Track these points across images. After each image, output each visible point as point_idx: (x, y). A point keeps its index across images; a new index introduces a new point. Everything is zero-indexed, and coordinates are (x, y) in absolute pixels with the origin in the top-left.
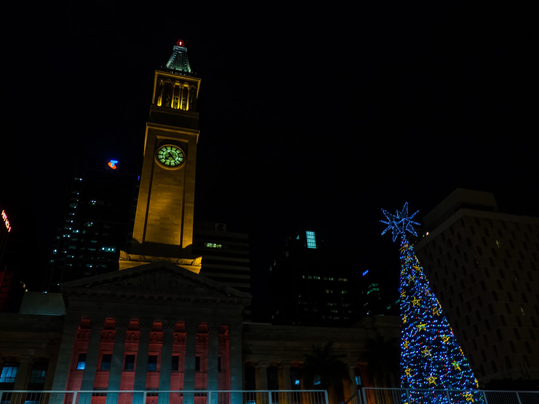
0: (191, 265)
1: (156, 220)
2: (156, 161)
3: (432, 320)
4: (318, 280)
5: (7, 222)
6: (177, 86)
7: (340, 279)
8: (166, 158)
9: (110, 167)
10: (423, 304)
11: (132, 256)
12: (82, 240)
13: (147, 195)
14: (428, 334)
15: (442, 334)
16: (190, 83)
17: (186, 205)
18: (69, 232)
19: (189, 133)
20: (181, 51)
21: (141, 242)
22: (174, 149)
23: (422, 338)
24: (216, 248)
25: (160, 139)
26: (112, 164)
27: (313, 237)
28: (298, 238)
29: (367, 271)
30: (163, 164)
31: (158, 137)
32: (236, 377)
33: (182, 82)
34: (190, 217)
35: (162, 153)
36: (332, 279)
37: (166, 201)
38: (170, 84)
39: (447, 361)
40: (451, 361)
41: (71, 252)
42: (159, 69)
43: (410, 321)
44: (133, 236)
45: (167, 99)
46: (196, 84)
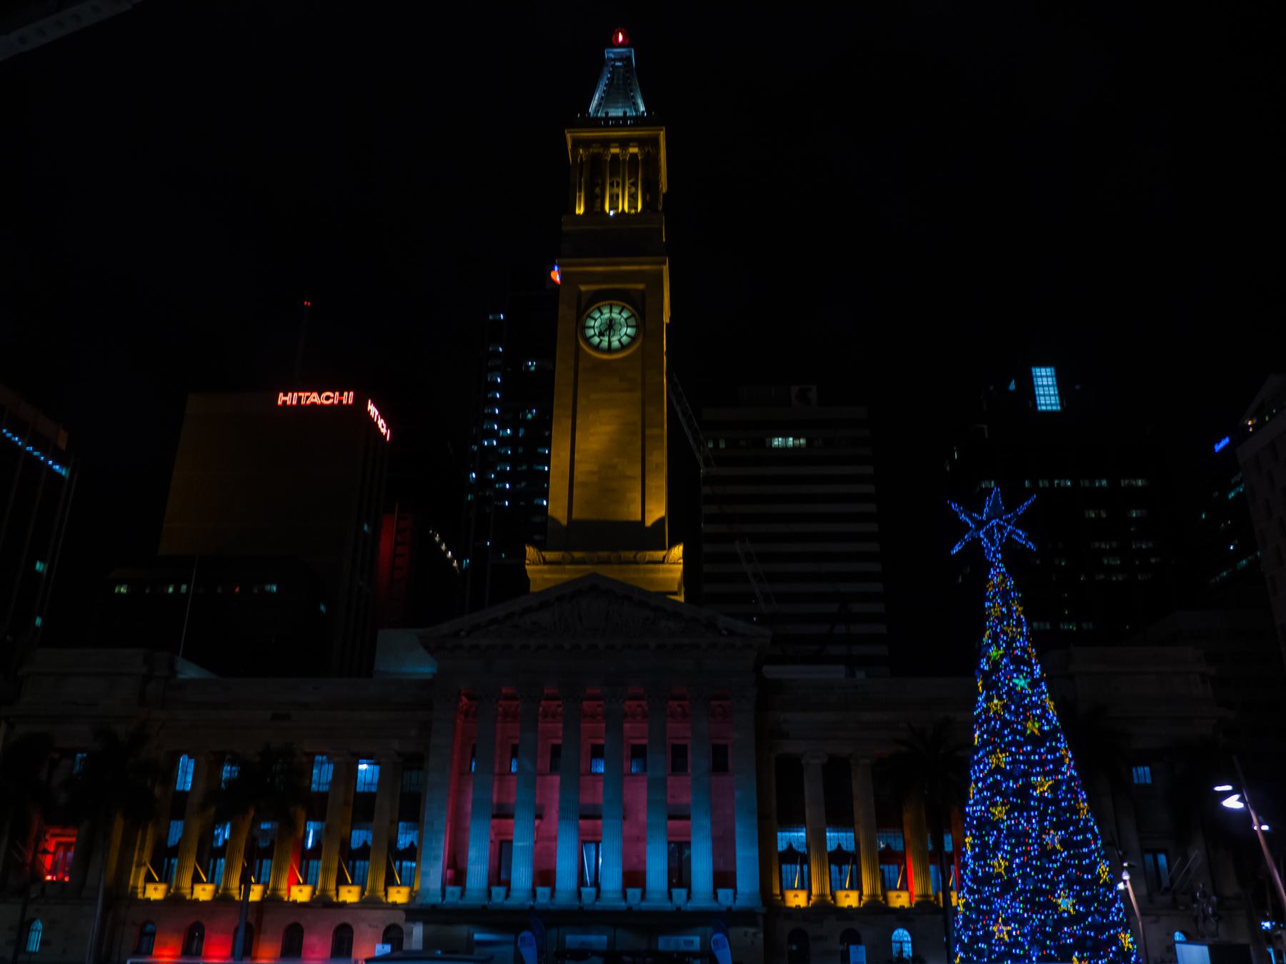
0: (663, 562)
3: (1019, 745)
4: (1066, 487)
5: (381, 422)
6: (615, 156)
7: (1124, 483)
8: (601, 334)
10: (1010, 712)
11: (549, 555)
12: (520, 450)
13: (569, 422)
14: (1007, 775)
15: (1037, 775)
16: (640, 142)
17: (648, 432)
18: (494, 434)
20: (620, 60)
21: (564, 522)
22: (616, 310)
23: (996, 782)
24: (794, 448)
25: (587, 292)
27: (1051, 381)
28: (1012, 386)
29: (1227, 440)
30: (597, 348)
31: (583, 288)
32: (742, 791)
33: (624, 143)
34: (659, 457)
35: (592, 323)
36: (1104, 483)
37: (607, 429)
39: (1034, 830)
40: (1044, 830)
41: (502, 477)
42: (574, 125)
43: (984, 743)
44: (550, 512)
45: (598, 190)
46: (654, 142)
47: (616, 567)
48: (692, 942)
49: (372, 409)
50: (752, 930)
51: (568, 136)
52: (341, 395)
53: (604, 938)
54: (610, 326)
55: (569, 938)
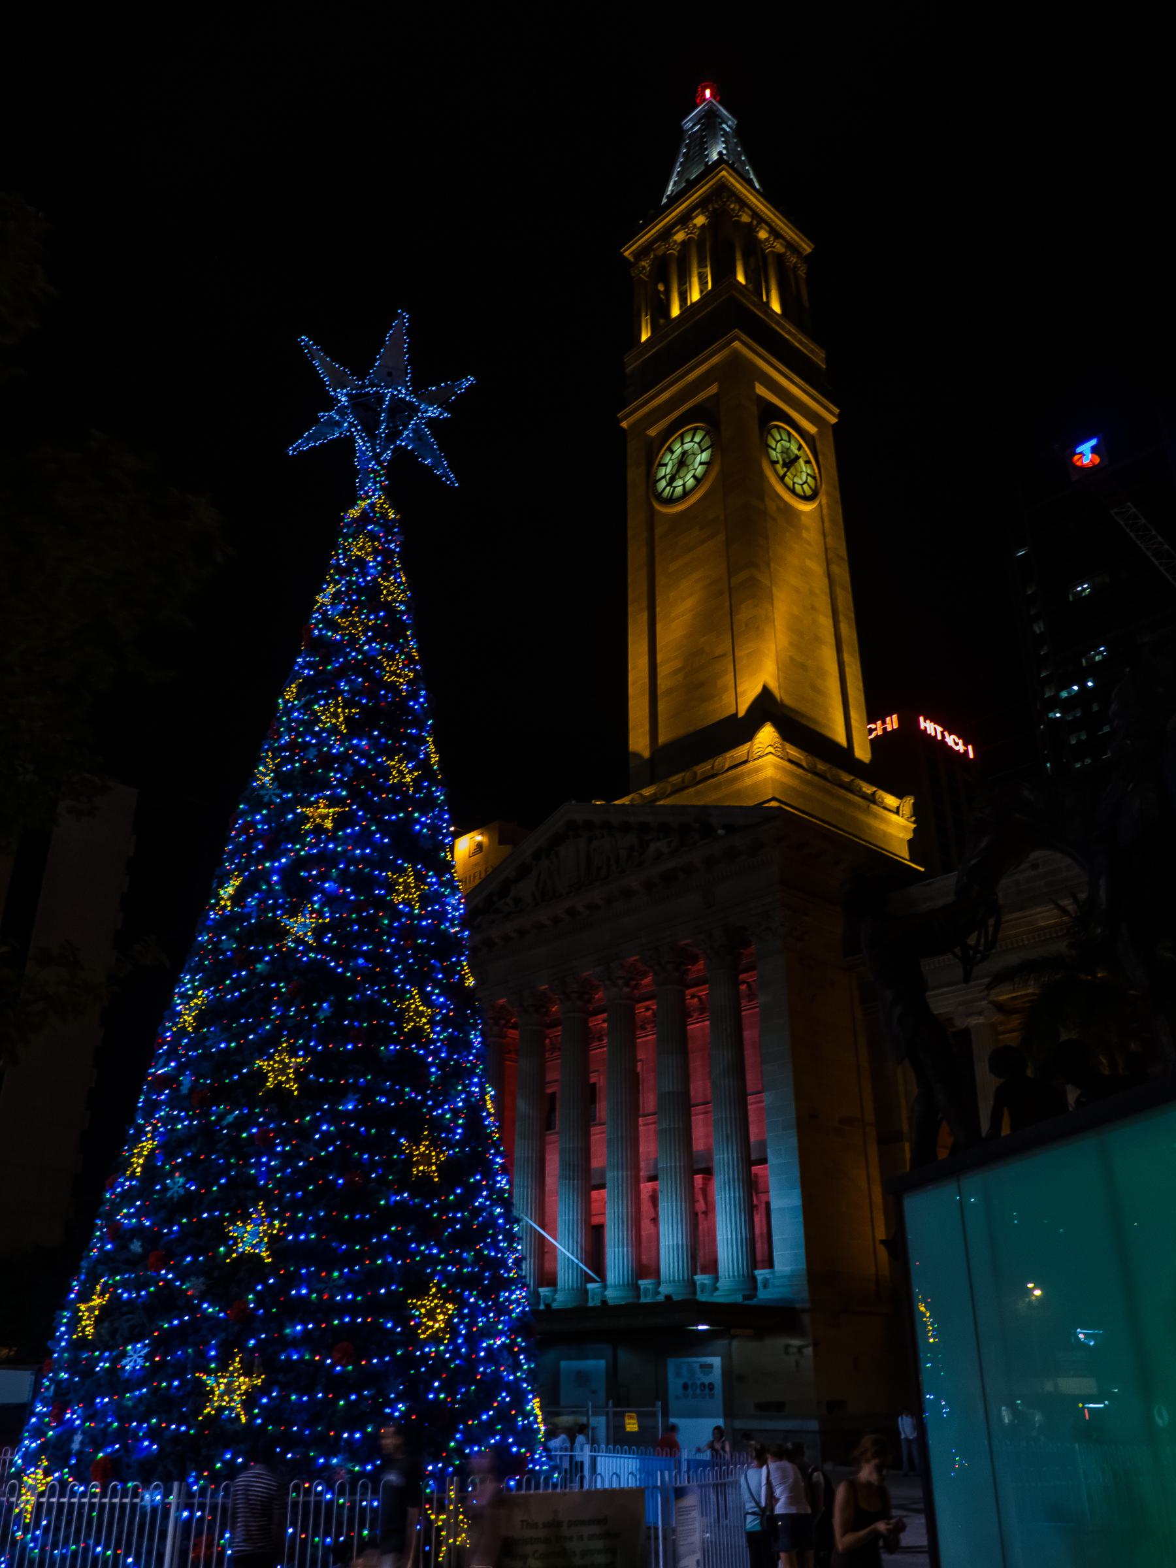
0: (746, 762)
1: (676, 672)
2: (657, 507)
5: (950, 740)
6: (683, 243)
9: (1083, 468)
12: (1095, 708)
13: (645, 615)
16: (702, 205)
19: (715, 360)
21: (646, 754)
26: (1086, 455)
31: (652, 432)
33: (684, 220)
37: (689, 603)
38: (665, 253)
47: (691, 790)
48: (711, 1366)
49: (930, 727)
50: (796, 1342)
51: (626, 254)
52: (884, 723)
53: (602, 1363)
54: (682, 463)
55: (563, 1364)
